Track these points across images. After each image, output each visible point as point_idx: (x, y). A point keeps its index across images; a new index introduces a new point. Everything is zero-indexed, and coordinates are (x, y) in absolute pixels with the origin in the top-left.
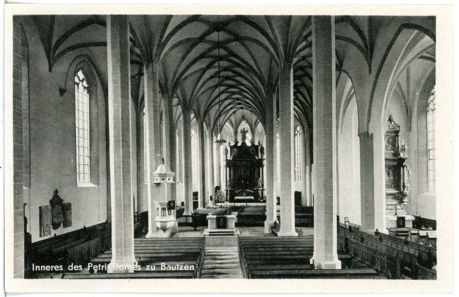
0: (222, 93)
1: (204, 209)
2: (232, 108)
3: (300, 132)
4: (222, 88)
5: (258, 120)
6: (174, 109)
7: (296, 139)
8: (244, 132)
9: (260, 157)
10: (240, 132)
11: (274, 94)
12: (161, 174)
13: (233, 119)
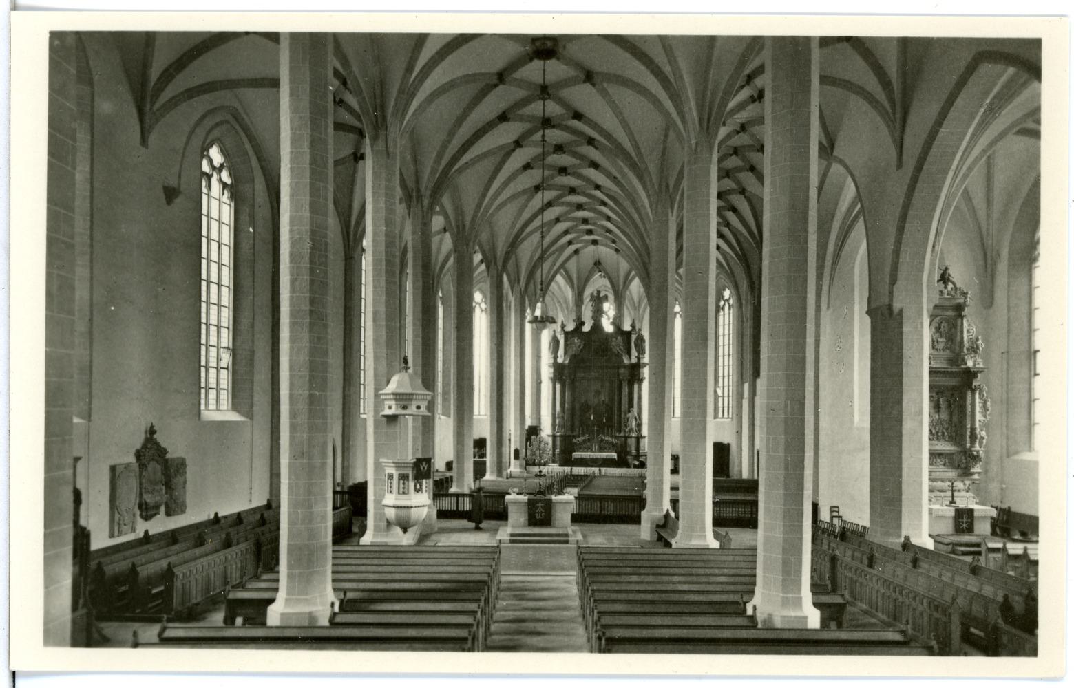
0: (549, 204)
1: (500, 479)
2: (570, 243)
3: (731, 302)
4: (549, 195)
5: (633, 273)
6: (435, 240)
7: (721, 318)
8: (598, 300)
9: (634, 360)
11: (672, 212)
12: (400, 394)
13: (572, 265)
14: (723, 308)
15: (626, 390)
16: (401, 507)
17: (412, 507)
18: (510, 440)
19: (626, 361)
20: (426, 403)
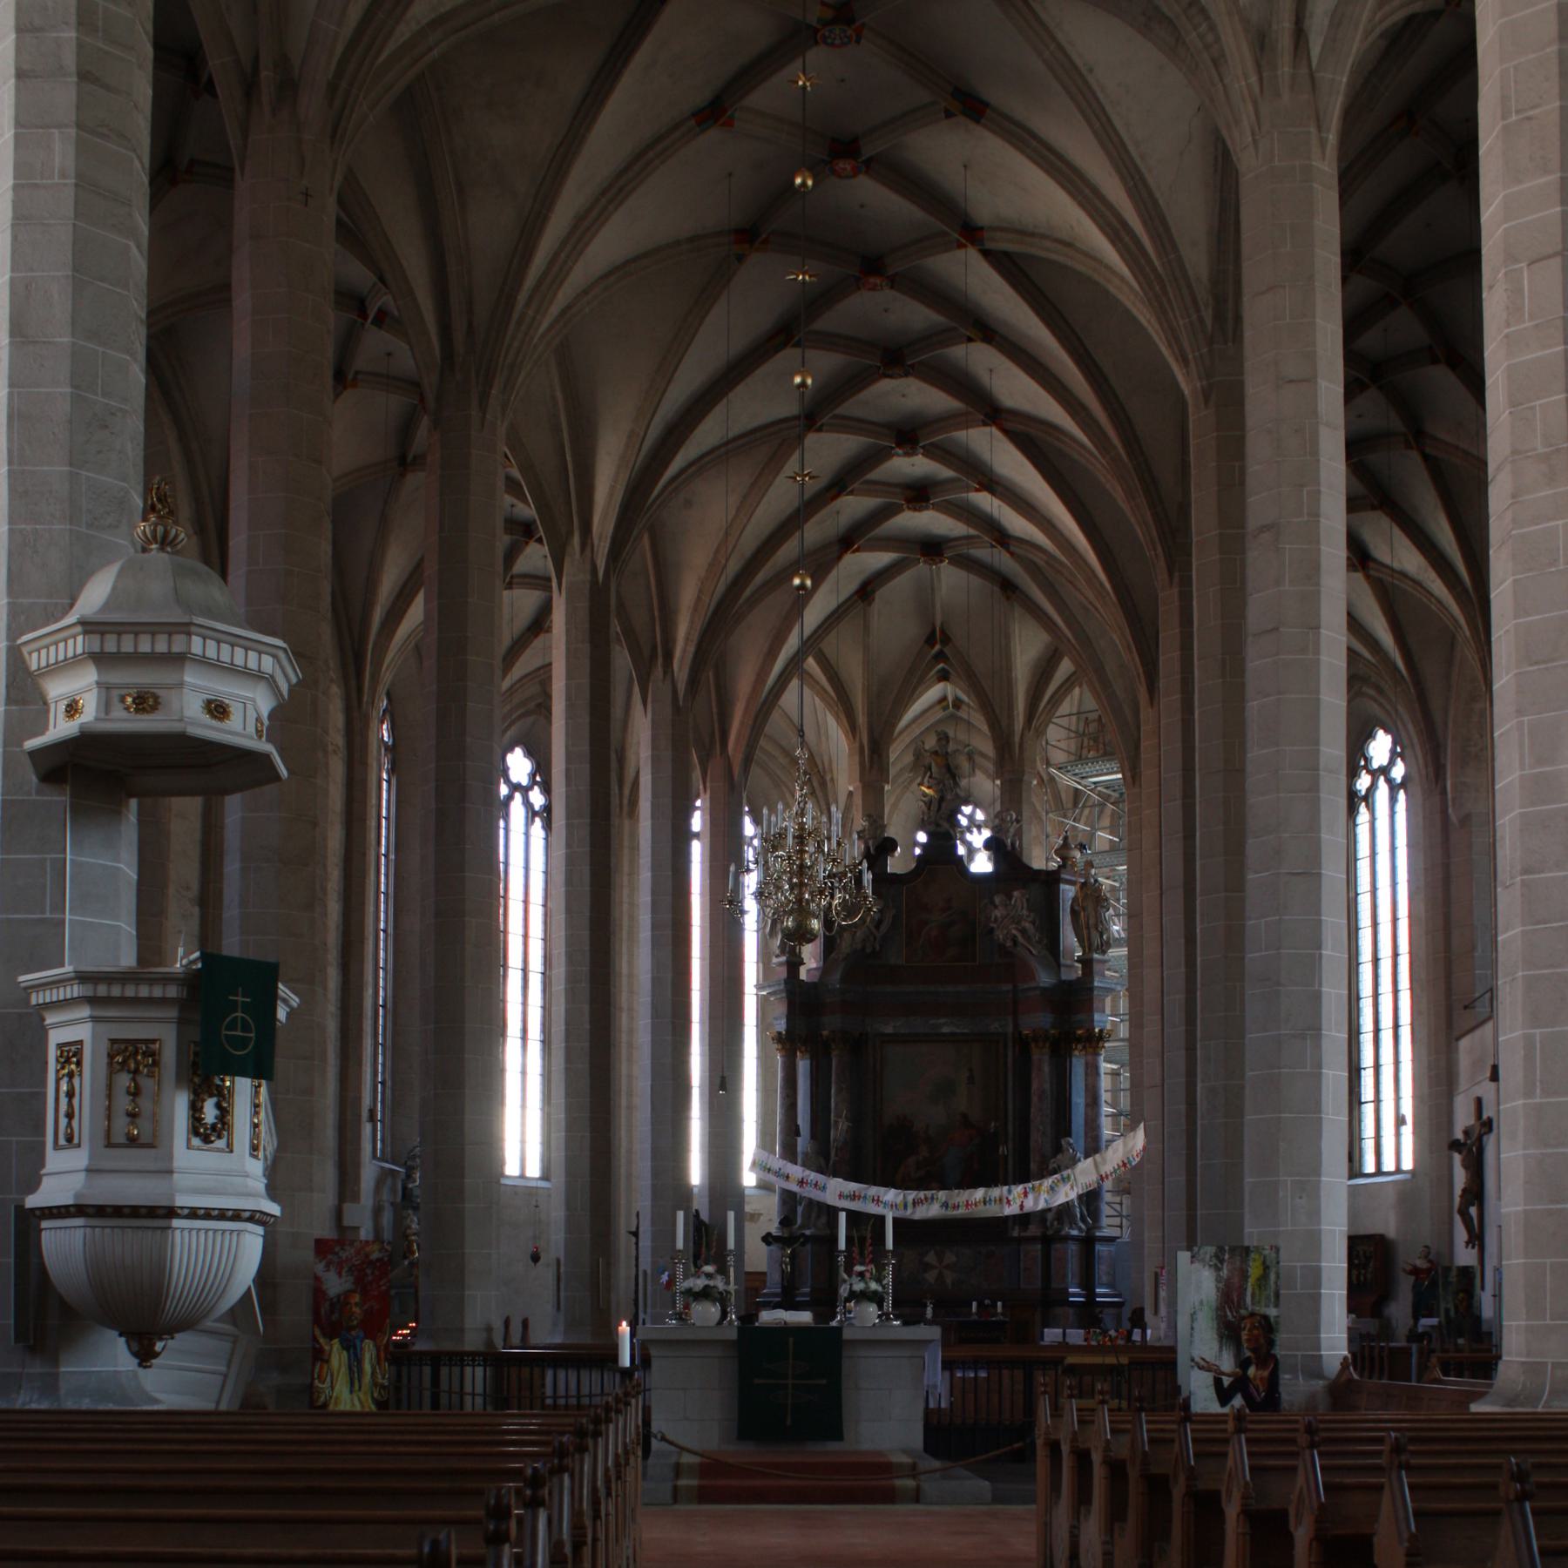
5: (1066, 667)
10: (909, 758)
14: (1368, 798)
15: (1042, 1079)
16: (117, 1211)
17: (171, 1212)
18: (636, 1234)
19: (1045, 979)
20: (264, 704)
